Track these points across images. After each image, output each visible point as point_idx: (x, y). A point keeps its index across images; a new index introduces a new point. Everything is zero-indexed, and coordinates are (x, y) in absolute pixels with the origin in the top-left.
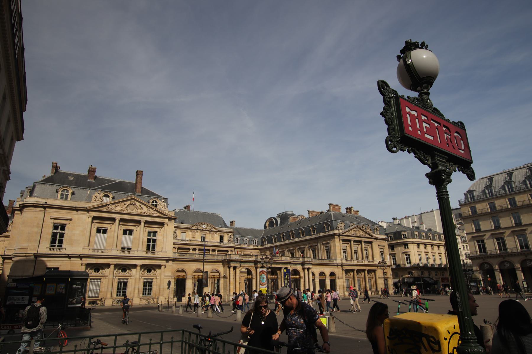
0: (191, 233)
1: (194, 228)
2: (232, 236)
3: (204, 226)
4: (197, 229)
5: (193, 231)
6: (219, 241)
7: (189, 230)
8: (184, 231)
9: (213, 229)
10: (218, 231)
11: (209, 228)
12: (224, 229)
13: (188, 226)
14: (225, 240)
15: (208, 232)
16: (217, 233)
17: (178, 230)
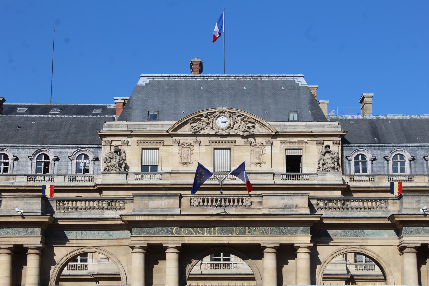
0: (175, 149)
1: (186, 129)
2: (336, 149)
3: (221, 123)
4: (195, 135)
5: (182, 140)
6: (283, 169)
7: (168, 141)
8: (150, 142)
9: (258, 129)
10: (276, 135)
11: (241, 128)
12: (303, 126)
13: (165, 125)
14: (309, 165)
15: (240, 142)
16: (277, 141)
17: (132, 141)
